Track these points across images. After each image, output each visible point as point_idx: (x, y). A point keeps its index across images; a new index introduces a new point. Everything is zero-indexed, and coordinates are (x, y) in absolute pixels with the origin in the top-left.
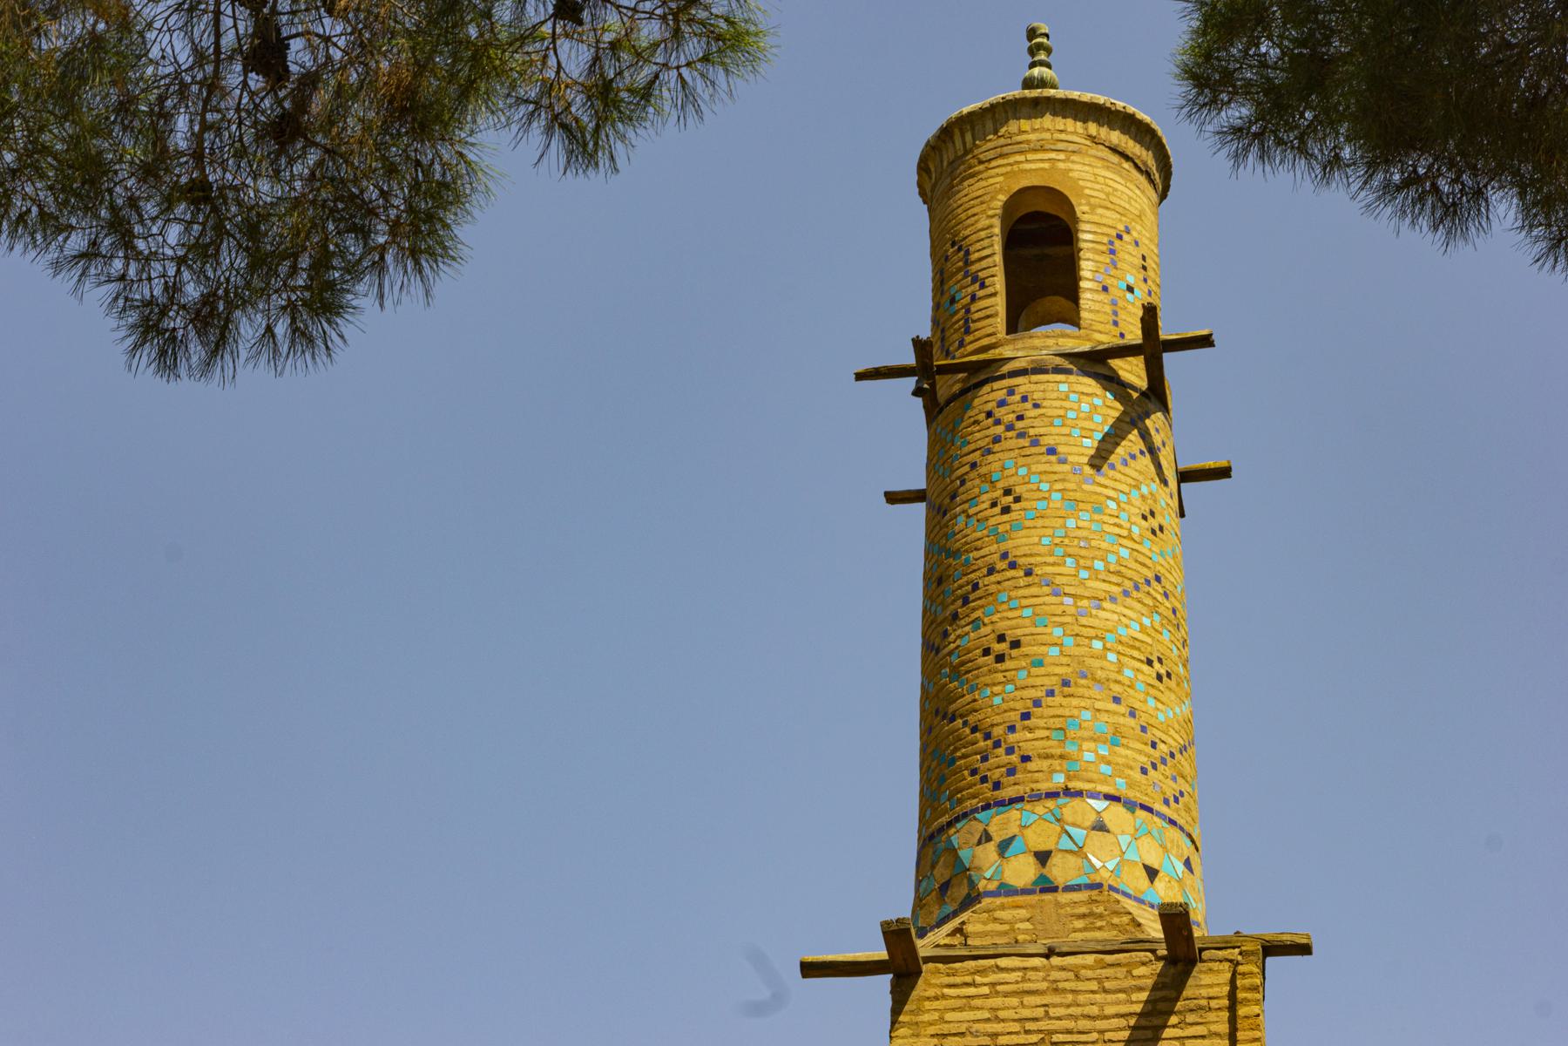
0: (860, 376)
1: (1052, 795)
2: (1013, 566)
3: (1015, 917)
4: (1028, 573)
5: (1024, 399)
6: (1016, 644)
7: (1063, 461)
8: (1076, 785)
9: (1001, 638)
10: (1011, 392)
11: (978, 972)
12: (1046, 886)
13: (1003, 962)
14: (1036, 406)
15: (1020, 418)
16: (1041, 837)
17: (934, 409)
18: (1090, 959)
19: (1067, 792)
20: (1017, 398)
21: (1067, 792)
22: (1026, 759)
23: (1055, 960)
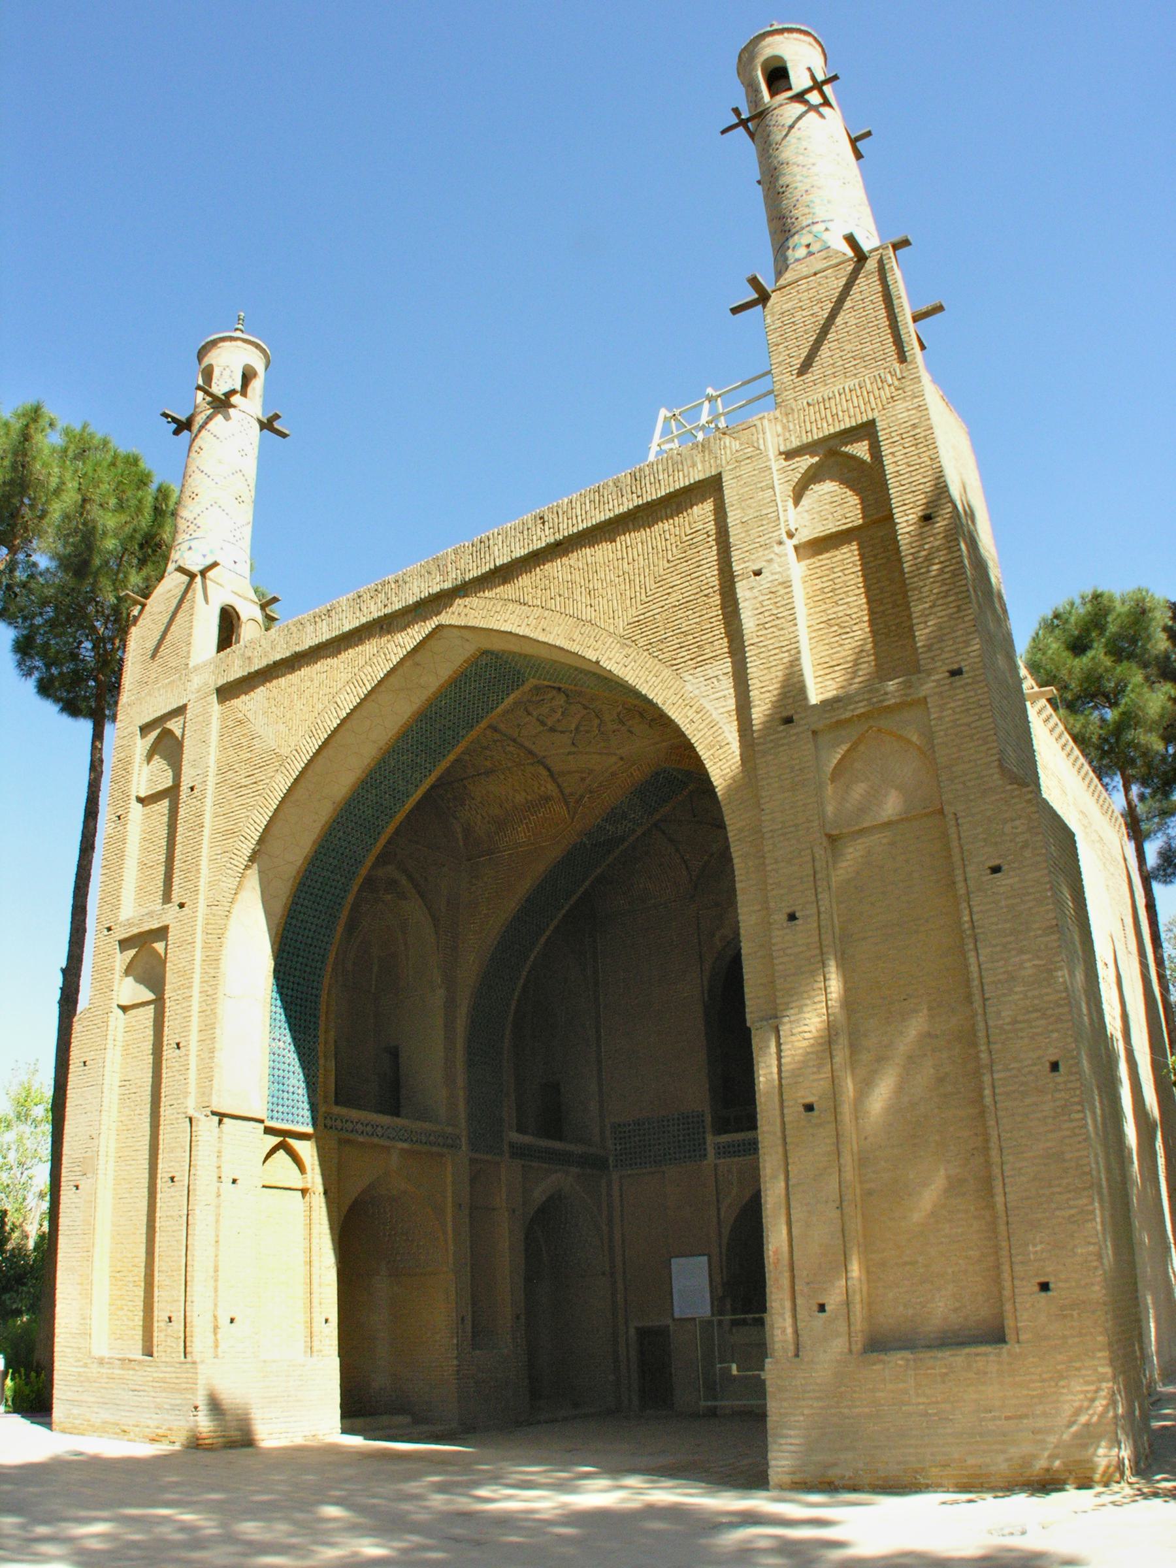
0: (723, 132)
3: (803, 269)
6: (787, 186)
11: (792, 289)
12: (811, 254)
13: (799, 283)
17: (752, 135)
18: (830, 271)
19: (813, 223)
21: (813, 223)
23: (818, 276)
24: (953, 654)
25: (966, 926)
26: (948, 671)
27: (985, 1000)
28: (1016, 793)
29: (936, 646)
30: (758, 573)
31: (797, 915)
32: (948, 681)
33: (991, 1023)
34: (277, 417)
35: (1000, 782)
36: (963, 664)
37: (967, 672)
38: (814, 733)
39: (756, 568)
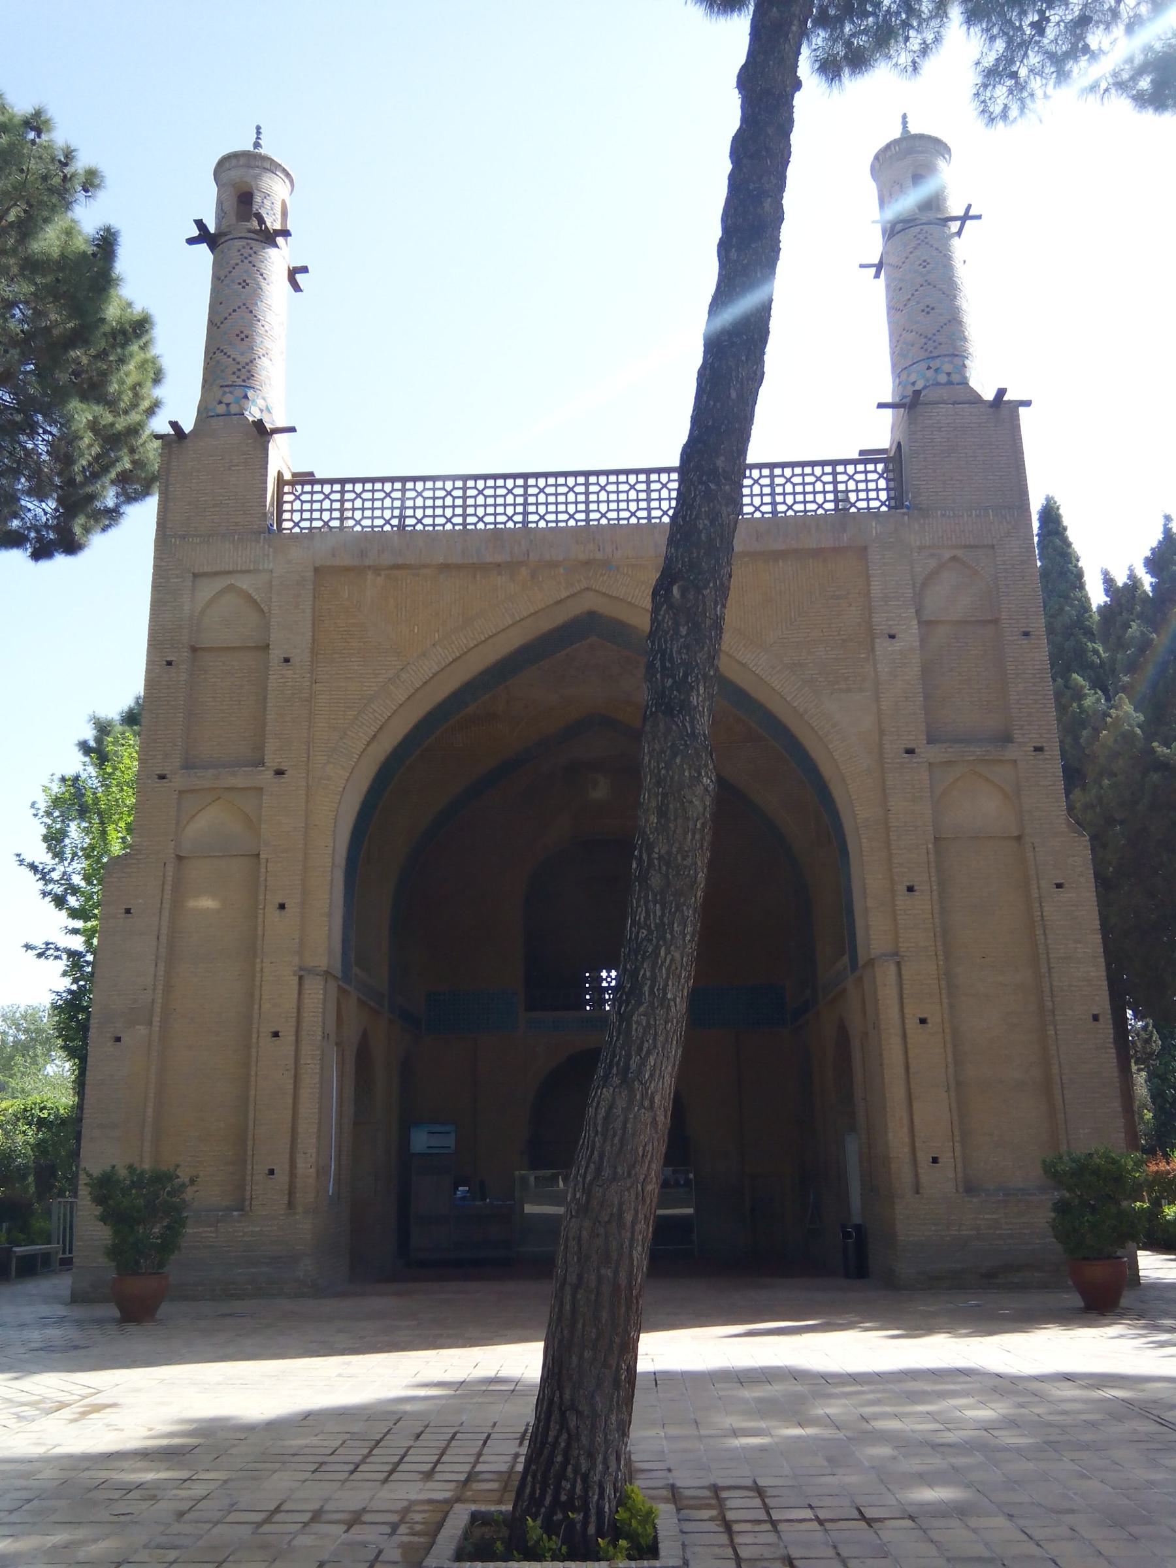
1: (948, 355)
2: (929, 284)
4: (935, 287)
5: (927, 232)
7: (941, 252)
8: (956, 353)
9: (928, 306)
10: (922, 230)
12: (950, 383)
14: (931, 235)
15: (926, 238)
16: (947, 367)
18: (967, 405)
20: (924, 231)
22: (940, 344)
23: (956, 406)
24: (1038, 736)
25: (1039, 918)
26: (1034, 747)
27: (1050, 969)
28: (1077, 839)
29: (1026, 727)
30: (892, 637)
31: (915, 888)
32: (1034, 754)
33: (1055, 984)
34: (304, 270)
35: (1066, 830)
36: (1044, 744)
37: (1047, 751)
38: (930, 764)
39: (892, 632)
